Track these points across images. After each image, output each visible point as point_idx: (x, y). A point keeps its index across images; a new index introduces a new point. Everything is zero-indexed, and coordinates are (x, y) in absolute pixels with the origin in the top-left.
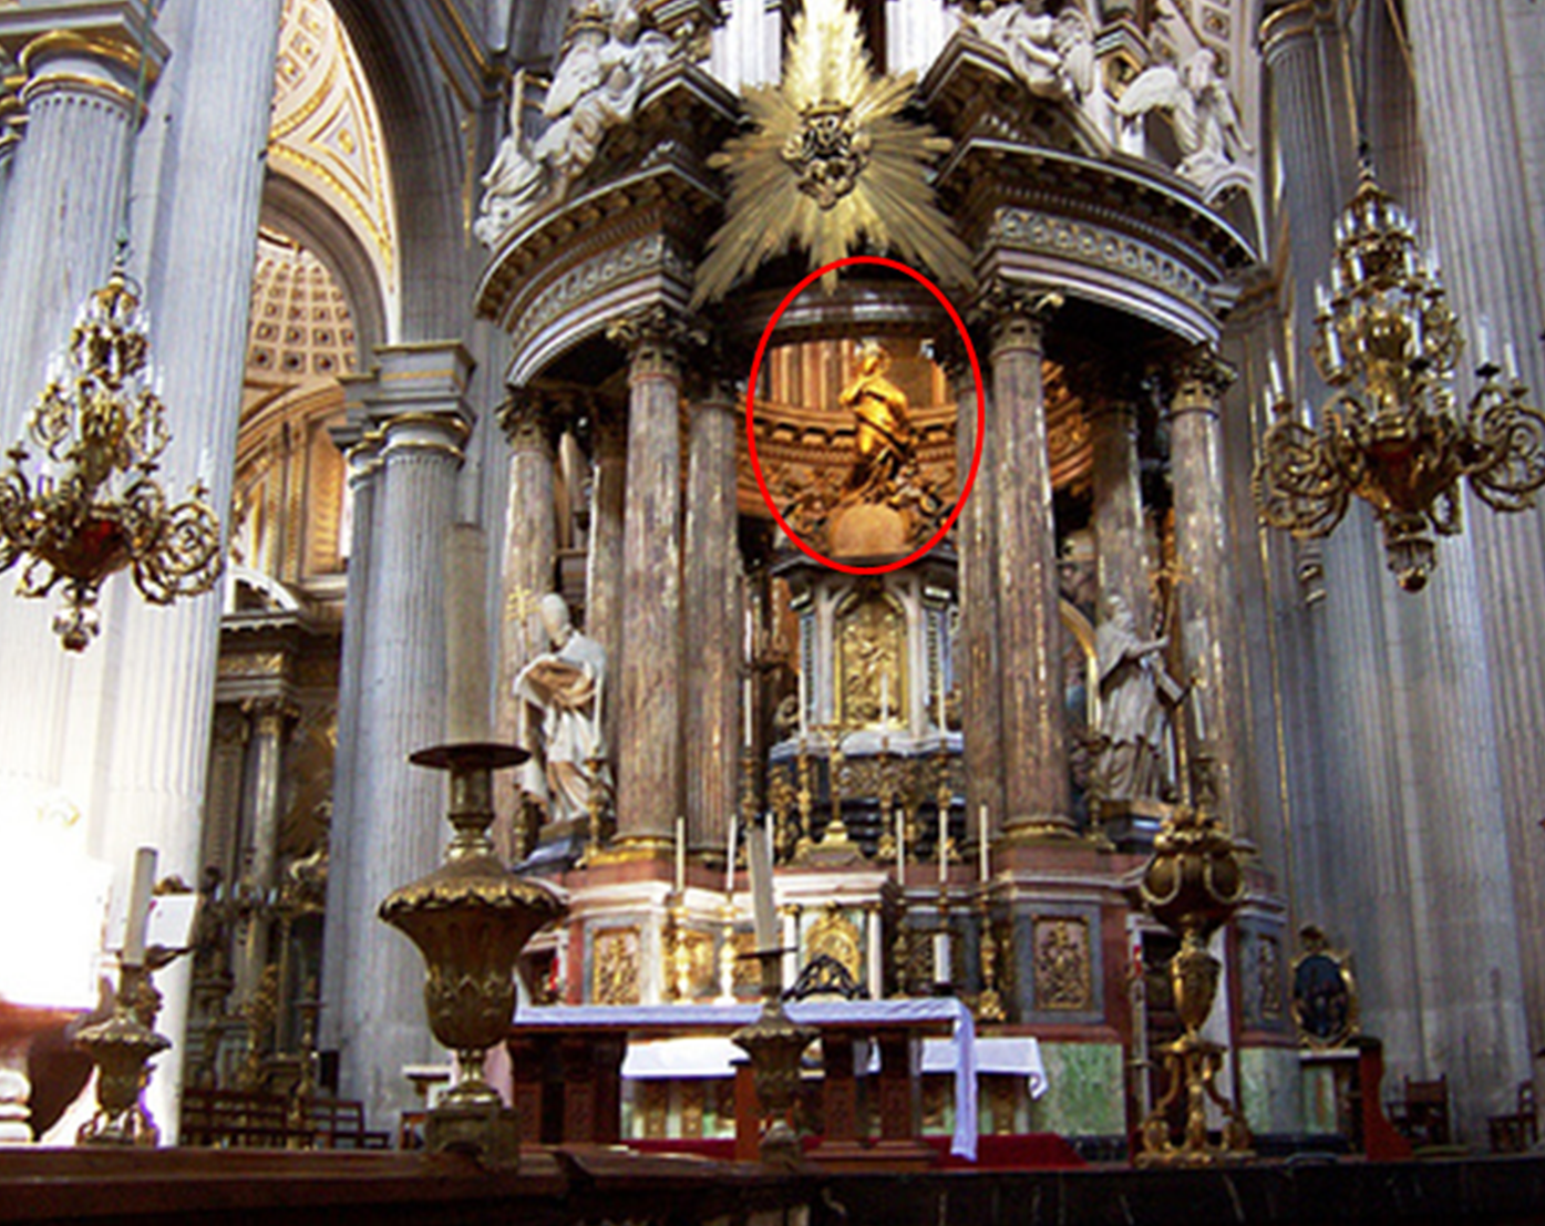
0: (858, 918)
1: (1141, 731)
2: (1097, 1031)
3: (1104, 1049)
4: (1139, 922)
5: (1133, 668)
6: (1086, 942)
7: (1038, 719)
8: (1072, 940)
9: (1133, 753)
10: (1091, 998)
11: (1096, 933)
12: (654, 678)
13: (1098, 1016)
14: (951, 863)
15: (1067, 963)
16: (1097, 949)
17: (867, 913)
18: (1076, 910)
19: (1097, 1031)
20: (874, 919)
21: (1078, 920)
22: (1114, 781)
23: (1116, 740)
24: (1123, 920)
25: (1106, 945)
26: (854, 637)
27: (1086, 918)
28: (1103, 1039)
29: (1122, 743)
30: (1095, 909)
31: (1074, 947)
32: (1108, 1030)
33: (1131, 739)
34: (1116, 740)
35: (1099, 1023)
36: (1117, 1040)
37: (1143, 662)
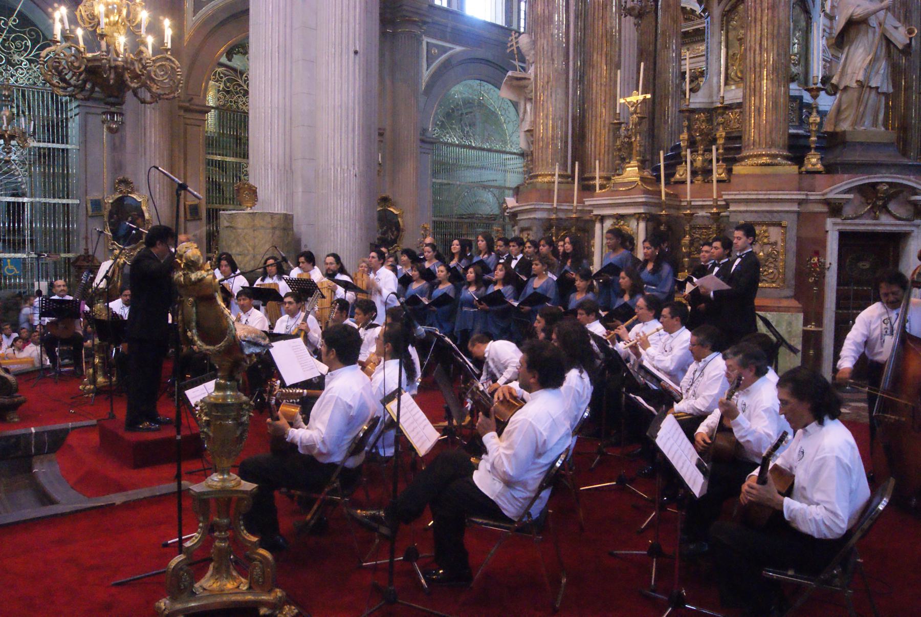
0: (633, 223)
1: (861, 77)
2: (785, 303)
3: (786, 316)
4: (835, 224)
5: (864, 27)
6: (784, 240)
7: (761, 79)
8: (772, 240)
9: (856, 94)
10: (784, 281)
11: (793, 233)
12: (546, 79)
13: (789, 292)
14: (719, 181)
15: (768, 255)
16: (793, 245)
17: (638, 220)
18: (776, 218)
19: (785, 303)
20: (642, 225)
21: (779, 225)
22: (843, 117)
23: (841, 87)
24: (825, 223)
25: (800, 241)
26: (735, 29)
27: (784, 223)
28: (787, 309)
29: (846, 88)
30: (795, 217)
31: (775, 243)
32: (794, 303)
33: (854, 85)
34: (841, 87)
35: (787, 298)
36: (797, 310)
37: (873, 22)
